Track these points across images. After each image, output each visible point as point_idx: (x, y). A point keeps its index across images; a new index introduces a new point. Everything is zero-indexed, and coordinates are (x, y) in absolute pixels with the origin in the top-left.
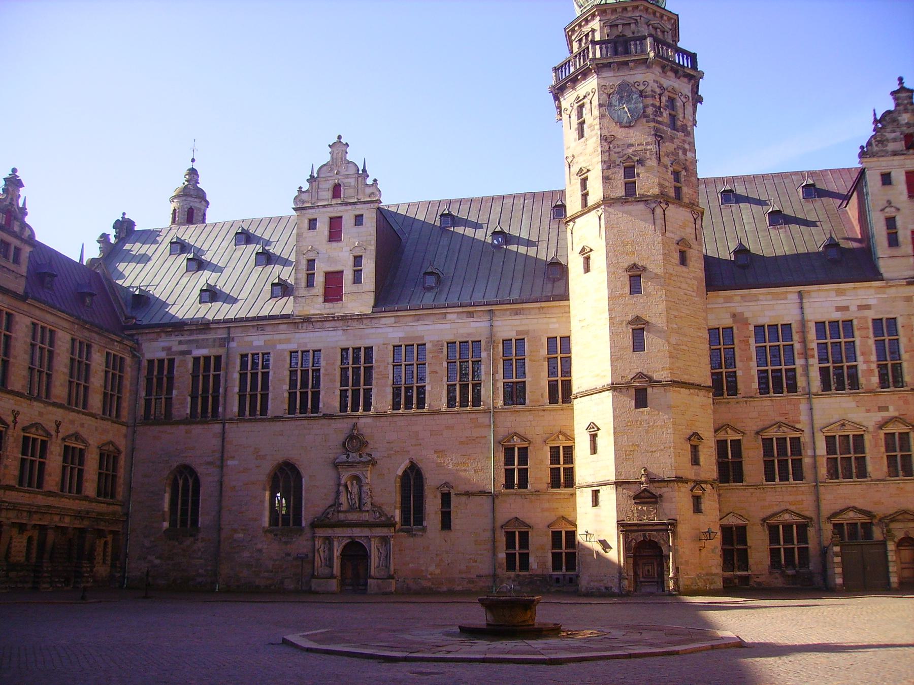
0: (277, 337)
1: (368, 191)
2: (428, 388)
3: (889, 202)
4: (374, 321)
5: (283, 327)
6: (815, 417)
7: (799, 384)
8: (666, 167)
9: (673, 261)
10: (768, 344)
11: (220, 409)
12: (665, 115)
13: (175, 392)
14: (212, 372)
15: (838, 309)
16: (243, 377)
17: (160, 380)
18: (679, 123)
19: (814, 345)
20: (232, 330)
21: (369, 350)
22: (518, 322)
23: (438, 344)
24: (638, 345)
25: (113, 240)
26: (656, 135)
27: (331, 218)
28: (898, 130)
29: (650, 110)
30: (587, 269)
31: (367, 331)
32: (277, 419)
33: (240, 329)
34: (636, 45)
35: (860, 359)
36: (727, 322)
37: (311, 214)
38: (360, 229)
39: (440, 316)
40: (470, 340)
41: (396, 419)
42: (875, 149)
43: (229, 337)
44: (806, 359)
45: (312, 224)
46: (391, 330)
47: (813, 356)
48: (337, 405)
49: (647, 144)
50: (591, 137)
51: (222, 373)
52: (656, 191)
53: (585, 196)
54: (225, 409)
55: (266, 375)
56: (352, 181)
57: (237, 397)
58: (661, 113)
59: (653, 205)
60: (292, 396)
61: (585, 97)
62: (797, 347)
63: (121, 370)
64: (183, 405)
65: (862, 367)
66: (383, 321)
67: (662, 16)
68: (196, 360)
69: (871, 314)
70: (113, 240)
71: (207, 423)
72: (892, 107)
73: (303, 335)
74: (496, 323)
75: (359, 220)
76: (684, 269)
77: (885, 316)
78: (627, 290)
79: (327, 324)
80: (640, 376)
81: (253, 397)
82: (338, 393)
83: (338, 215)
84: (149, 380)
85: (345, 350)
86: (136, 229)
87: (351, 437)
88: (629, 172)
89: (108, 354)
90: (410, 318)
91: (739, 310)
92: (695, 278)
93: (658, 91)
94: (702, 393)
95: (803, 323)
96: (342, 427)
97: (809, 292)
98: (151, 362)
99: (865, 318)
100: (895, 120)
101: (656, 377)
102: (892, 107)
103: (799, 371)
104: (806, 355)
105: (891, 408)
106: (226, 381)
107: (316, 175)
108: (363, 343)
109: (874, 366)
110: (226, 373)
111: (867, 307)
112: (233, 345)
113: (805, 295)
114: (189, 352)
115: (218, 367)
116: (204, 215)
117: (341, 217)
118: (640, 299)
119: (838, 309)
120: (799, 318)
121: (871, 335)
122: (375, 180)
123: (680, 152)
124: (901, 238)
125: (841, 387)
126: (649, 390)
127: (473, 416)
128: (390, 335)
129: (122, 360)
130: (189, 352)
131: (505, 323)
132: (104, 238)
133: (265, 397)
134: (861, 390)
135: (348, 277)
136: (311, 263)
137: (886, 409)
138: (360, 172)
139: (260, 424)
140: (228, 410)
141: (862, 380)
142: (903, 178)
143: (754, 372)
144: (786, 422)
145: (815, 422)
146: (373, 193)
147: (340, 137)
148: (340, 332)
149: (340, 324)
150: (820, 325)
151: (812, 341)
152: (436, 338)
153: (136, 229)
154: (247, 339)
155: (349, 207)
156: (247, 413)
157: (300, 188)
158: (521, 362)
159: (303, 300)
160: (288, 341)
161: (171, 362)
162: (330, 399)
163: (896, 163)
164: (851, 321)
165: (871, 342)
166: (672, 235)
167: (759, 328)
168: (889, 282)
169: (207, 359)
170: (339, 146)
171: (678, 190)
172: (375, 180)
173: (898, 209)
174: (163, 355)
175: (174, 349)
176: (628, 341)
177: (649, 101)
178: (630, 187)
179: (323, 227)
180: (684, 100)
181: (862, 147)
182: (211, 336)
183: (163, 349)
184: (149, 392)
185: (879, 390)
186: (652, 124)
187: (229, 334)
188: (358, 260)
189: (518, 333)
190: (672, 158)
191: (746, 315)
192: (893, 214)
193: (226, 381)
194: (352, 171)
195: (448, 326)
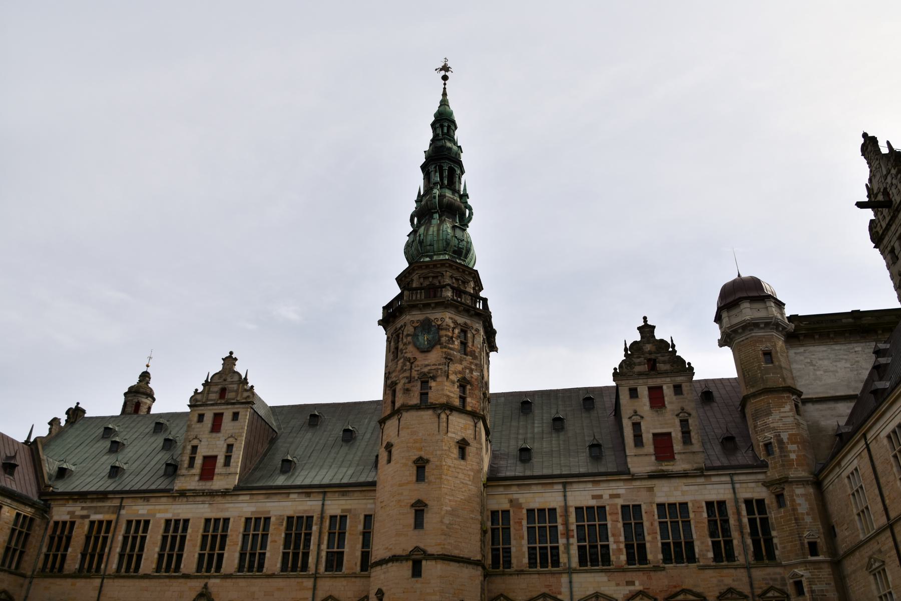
0: (158, 507)
1: (246, 394)
2: (268, 555)
3: (635, 412)
4: (234, 498)
5: (164, 500)
6: (574, 589)
7: (561, 560)
8: (453, 382)
9: (453, 455)
10: (537, 525)
11: (103, 566)
12: (456, 343)
13: (70, 550)
14: (102, 534)
15: (594, 497)
16: (125, 538)
17: (60, 539)
18: (469, 349)
20: (125, 501)
21: (226, 520)
22: (343, 502)
23: (280, 518)
24: (419, 523)
25: (63, 423)
26: (446, 358)
29: (444, 339)
30: (389, 461)
31: (228, 505)
32: (146, 576)
33: (130, 500)
35: (611, 539)
36: (506, 506)
37: (201, 410)
38: (236, 423)
39: (285, 495)
40: (305, 515)
41: (239, 580)
42: (625, 370)
43: (121, 505)
44: (568, 540)
45: (201, 417)
46: (245, 505)
47: (573, 537)
48: (194, 566)
49: (439, 365)
51: (110, 535)
52: (443, 400)
53: (393, 402)
54: (106, 566)
55: (143, 539)
56: (235, 386)
57: (117, 556)
58: (453, 342)
59: (439, 412)
60: (161, 556)
61: (400, 329)
62: (560, 528)
63: (29, 528)
64: (73, 561)
65: (613, 546)
66: (241, 498)
67: (464, 271)
68: (92, 523)
69: (620, 502)
70: (63, 423)
71: (89, 577)
72: (638, 338)
73: (178, 506)
74: (327, 502)
75: (235, 416)
76: (462, 462)
77: (631, 503)
78: (414, 478)
79: (198, 499)
80: (417, 549)
81: (130, 557)
82: (196, 556)
84: (52, 538)
85: (208, 521)
86: (86, 415)
87: (201, 595)
89: (18, 515)
90: (261, 497)
91: (515, 496)
92: (472, 470)
93: (452, 325)
94: (470, 567)
95: (566, 508)
96: (197, 585)
98: (56, 523)
99: (616, 505)
101: (431, 550)
102: (638, 338)
103: (561, 549)
104: (568, 536)
105: (637, 583)
106: (112, 542)
108: (221, 515)
109: (622, 546)
110: (113, 536)
111: (618, 496)
112: (123, 512)
114: (88, 517)
115: (107, 531)
116: (149, 408)
117: (222, 414)
118: (422, 486)
119: (594, 497)
120: (563, 504)
121: (620, 519)
122: (252, 387)
123: (467, 371)
124: (644, 440)
125: (594, 562)
126: (424, 563)
127: (300, 580)
128: (245, 509)
129: (32, 520)
130: (88, 517)
131: (334, 502)
132: (54, 422)
133: (139, 557)
134: (611, 567)
135: (221, 460)
136: (195, 449)
137: (633, 583)
139: (131, 580)
140: (109, 567)
141: (613, 558)
143: (525, 549)
144: (550, 593)
145: (574, 594)
146: (248, 397)
147: (231, 353)
148: (207, 506)
149: (207, 499)
150: (579, 510)
152: (279, 513)
153: (86, 415)
154: (134, 507)
156: (123, 570)
157: (196, 390)
158: (342, 535)
159: (182, 479)
160: (166, 511)
161: (73, 524)
162: (189, 562)
163: (641, 381)
164: (604, 507)
165: (620, 525)
166: (454, 435)
167: (530, 511)
168: (634, 478)
169: (101, 522)
170: (230, 361)
171: (463, 399)
173: (642, 417)
174: (67, 518)
175: (77, 513)
176: (411, 521)
177: (443, 333)
178: (424, 395)
180: (475, 333)
181: (615, 369)
182: (108, 504)
183: (69, 513)
184: (49, 549)
185: (626, 566)
186: (444, 350)
187: (121, 503)
188: (230, 447)
189: (343, 511)
190: (459, 376)
191: (521, 501)
193: (112, 542)
194: (236, 378)
195: (290, 503)
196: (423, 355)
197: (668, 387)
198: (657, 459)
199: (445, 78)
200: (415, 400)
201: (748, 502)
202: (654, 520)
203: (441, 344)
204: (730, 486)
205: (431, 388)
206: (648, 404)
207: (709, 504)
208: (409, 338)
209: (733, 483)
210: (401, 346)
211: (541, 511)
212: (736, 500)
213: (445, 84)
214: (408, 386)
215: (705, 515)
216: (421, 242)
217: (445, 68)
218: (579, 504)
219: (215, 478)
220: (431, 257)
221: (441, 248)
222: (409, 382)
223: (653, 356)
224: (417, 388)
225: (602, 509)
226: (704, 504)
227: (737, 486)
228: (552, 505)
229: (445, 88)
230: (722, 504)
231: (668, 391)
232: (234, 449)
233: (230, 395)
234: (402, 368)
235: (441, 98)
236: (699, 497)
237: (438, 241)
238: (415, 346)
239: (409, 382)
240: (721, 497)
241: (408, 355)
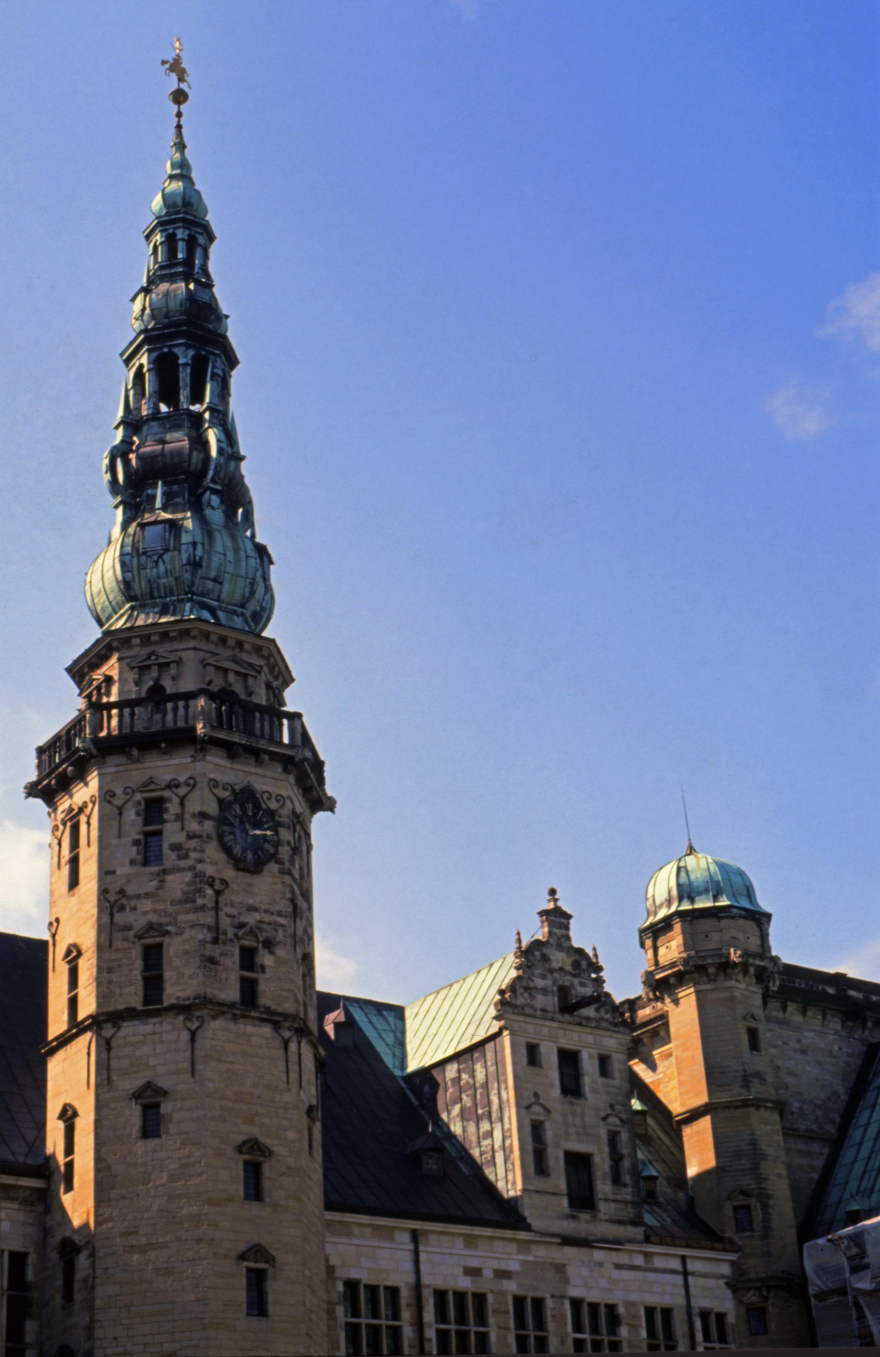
3: (536, 1095)
19: (430, 1333)
28: (549, 976)
34: (262, 721)
42: (520, 1001)
49: (279, 913)
50: (181, 870)
59: (287, 1034)
69: (511, 1287)
77: (530, 1294)
88: (248, 959)
95: (418, 1288)
97: (426, 1232)
99: (503, 1293)
100: (545, 958)
113: (421, 1239)
120: (411, 1279)
121: (512, 1324)
142: (554, 1058)
150: (440, 1295)
151: (430, 1326)
163: (545, 1031)
173: (548, 1111)
192: (542, 1118)
196: (242, 877)
197: (591, 1056)
198: (572, 1205)
200: (232, 993)
201: (705, 1315)
202: (567, 1334)
203: (280, 862)
204: (679, 1279)
205: (263, 968)
206: (557, 1083)
207: (650, 1311)
209: (685, 1273)
210: (172, 833)
211: (373, 1290)
212: (689, 1308)
213: (179, 115)
214: (211, 950)
215: (644, 1333)
217: (176, 67)
218: (440, 1283)
220: (212, 611)
221: (237, 598)
222: (215, 941)
223: (566, 980)
225: (480, 1299)
226: (642, 1312)
227: (691, 1279)
228: (391, 1281)
229: (179, 127)
230: (667, 1313)
231: (589, 1065)
234: (187, 899)
236: (634, 1297)
239: (215, 941)
240: (657, 1299)
241: (209, 870)
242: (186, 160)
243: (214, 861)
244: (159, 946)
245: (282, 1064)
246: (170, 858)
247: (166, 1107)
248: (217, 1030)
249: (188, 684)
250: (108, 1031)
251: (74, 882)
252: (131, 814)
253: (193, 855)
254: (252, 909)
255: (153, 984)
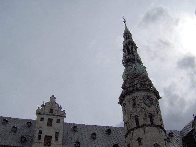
1: (62, 113)
27: (48, 119)
45: (42, 119)
49: (155, 112)
56: (57, 109)
59: (159, 128)
75: (58, 121)
83: (52, 118)
107: (44, 105)
117: (52, 119)
122: (64, 110)
135: (53, 138)
136: (40, 132)
138: (59, 107)
146: (63, 114)
147: (53, 95)
155: (55, 117)
157: (39, 108)
159: (35, 143)
170: (53, 98)
172: (64, 110)
178: (152, 122)
179: (46, 120)
188: (57, 133)
199: (125, 22)
200: (149, 123)
205: (153, 119)
208: (142, 101)
210: (137, 103)
216: (135, 69)
219: (51, 145)
221: (142, 72)
222: (146, 116)
224: (149, 118)
232: (59, 134)
233: (54, 112)
235: (124, 28)
237: (141, 70)
238: (145, 103)
239: (146, 116)
241: (143, 107)
242: (127, 28)
243: (143, 105)
244: (138, 118)
245: (159, 132)
246: (137, 106)
247: (142, 141)
248: (147, 128)
249: (136, 83)
250: (132, 132)
251: (125, 114)
252: (131, 102)
253: (140, 105)
254: (150, 111)
255: (137, 123)
